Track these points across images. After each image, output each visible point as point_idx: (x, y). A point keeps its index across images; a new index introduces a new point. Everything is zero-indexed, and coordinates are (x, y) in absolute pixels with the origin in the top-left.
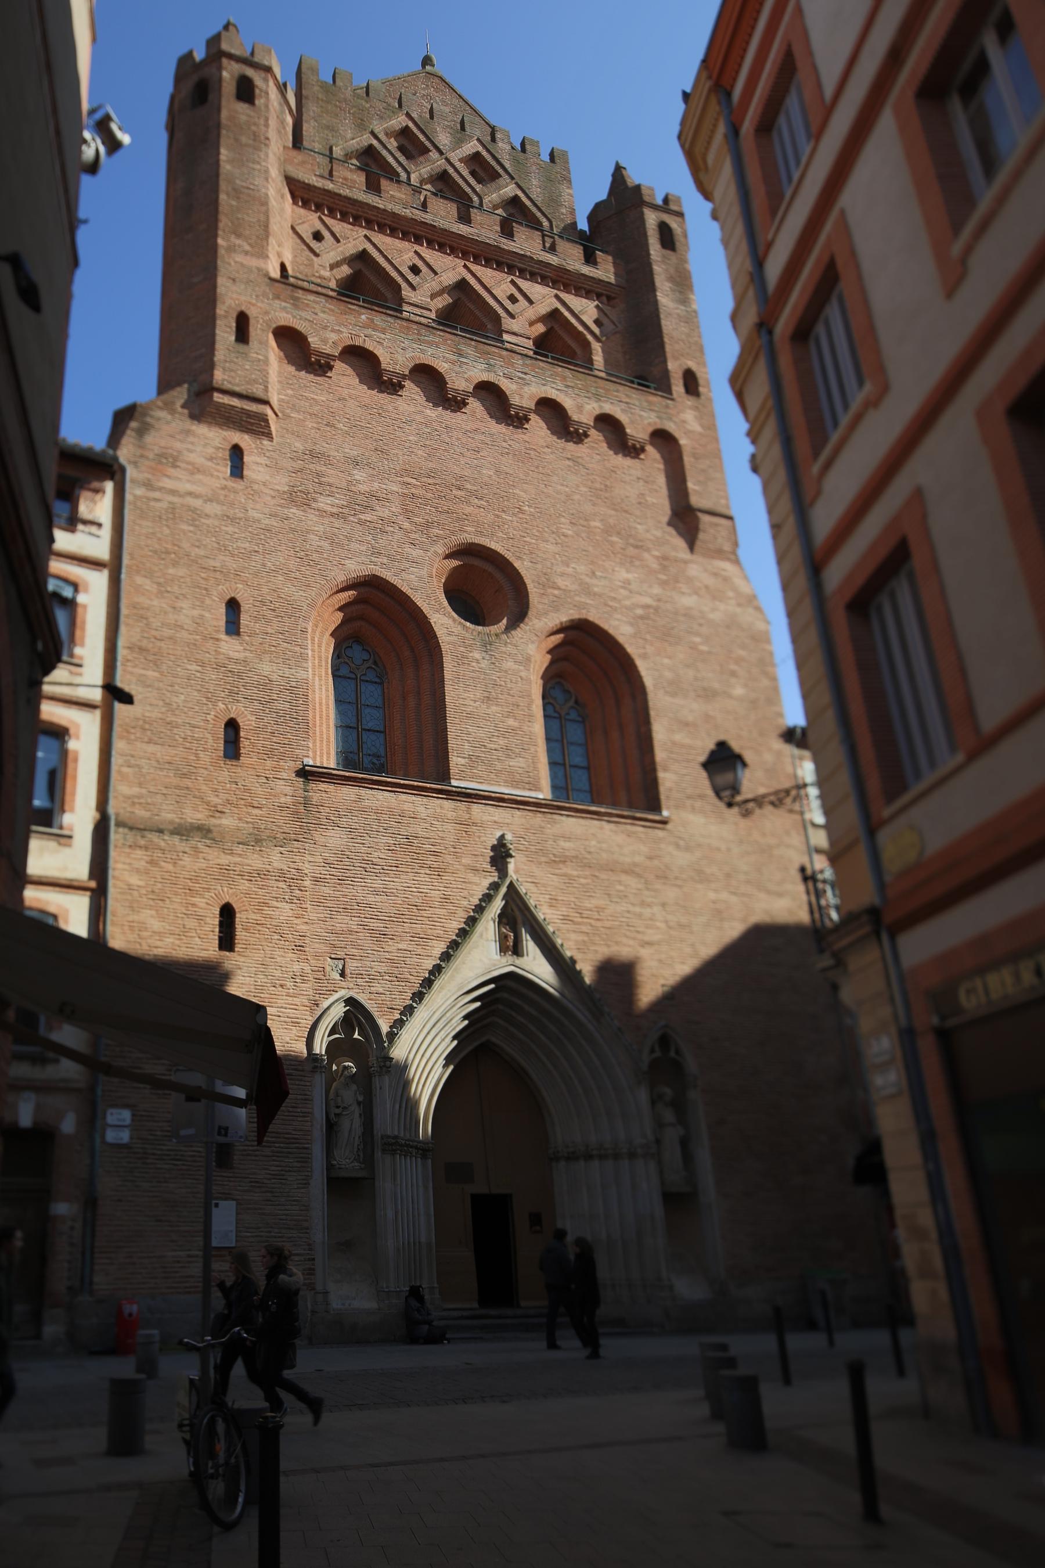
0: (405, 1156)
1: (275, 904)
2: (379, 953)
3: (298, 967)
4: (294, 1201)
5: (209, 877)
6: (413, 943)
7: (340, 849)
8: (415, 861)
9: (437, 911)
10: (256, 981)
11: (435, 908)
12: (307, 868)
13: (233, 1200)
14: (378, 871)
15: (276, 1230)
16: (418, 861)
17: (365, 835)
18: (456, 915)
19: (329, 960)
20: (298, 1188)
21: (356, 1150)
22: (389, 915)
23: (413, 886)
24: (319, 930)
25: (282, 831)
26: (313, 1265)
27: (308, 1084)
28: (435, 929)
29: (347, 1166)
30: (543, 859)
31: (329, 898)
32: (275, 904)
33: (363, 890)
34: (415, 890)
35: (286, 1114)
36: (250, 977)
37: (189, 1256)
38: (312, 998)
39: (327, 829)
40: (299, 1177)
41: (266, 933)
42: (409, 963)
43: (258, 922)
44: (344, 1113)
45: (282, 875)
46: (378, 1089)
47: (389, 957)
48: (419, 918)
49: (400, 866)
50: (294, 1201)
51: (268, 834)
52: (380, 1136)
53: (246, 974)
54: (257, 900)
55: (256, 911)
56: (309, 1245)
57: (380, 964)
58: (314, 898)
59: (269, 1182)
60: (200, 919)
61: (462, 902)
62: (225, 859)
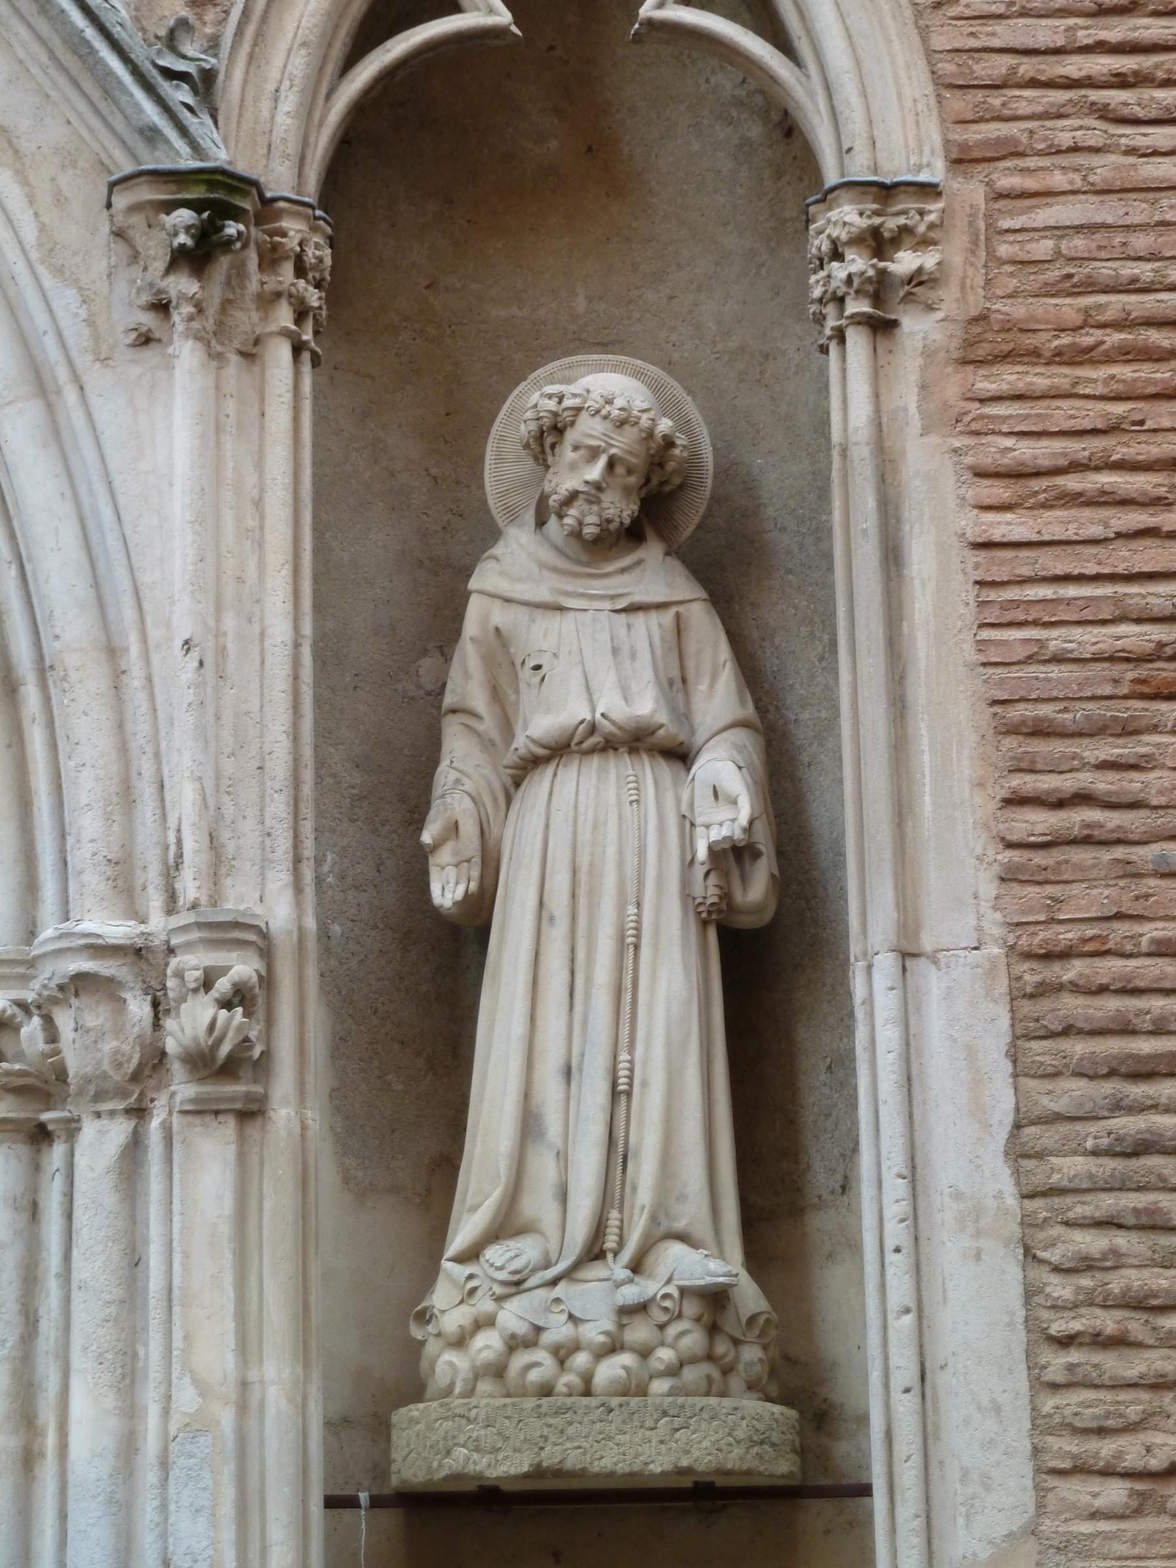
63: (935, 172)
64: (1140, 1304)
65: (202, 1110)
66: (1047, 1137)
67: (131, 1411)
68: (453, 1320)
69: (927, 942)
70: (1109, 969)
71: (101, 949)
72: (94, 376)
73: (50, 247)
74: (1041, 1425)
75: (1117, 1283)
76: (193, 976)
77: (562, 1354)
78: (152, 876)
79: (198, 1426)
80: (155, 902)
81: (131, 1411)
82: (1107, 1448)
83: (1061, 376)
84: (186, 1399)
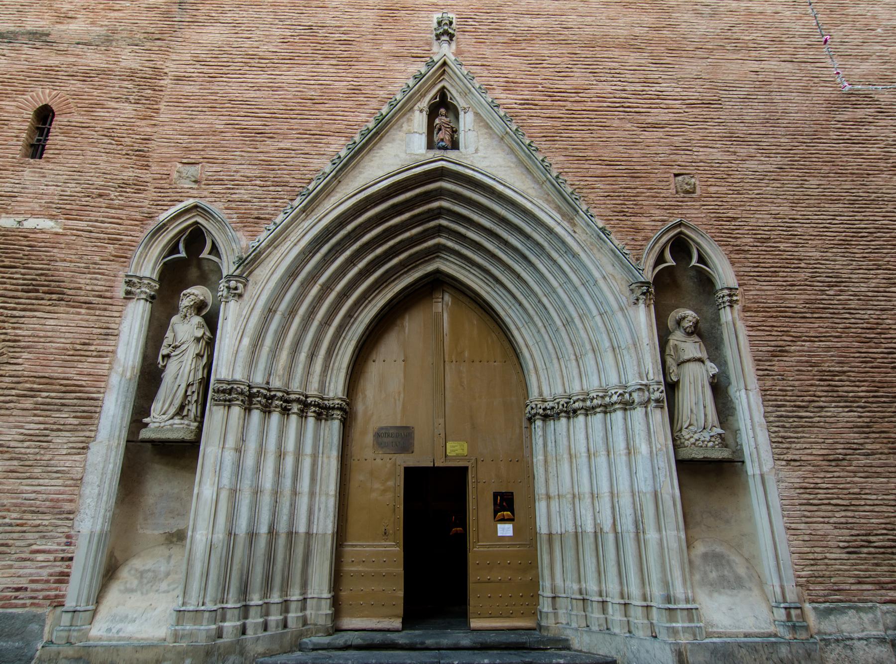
2: (249, 154)
3: (131, 174)
4: (56, 472)
5: (28, 79)
8: (318, 52)
9: (341, 104)
10: (63, 191)
11: (338, 100)
12: (171, 68)
15: (14, 515)
16: (321, 52)
17: (253, 29)
18: (366, 107)
19: (180, 165)
20: (69, 454)
22: (272, 111)
23: (311, 78)
24: (171, 133)
25: (143, 31)
26: (69, 567)
29: (162, 425)
30: (501, 39)
31: (192, 98)
33: (240, 86)
34: (312, 82)
35: (71, 353)
36: (57, 186)
38: (145, 210)
42: (291, 163)
44: (173, 354)
45: (131, 75)
48: (312, 113)
49: (296, 58)
50: (56, 472)
53: (50, 183)
54: (87, 101)
55: (83, 113)
56: (68, 537)
57: (250, 167)
59: (20, 445)
61: (377, 92)
63: (737, 287)
64: (783, 437)
65: (656, 407)
66: (768, 415)
67: (651, 448)
68: (687, 437)
69: (749, 388)
70: (773, 392)
71: (642, 385)
72: (628, 308)
73: (621, 292)
74: (773, 453)
75: (780, 434)
76: (656, 389)
77: (703, 442)
78: (644, 375)
79: (660, 450)
80: (645, 379)
81: (651, 448)
82: (782, 457)
83: (756, 314)
84: (659, 446)
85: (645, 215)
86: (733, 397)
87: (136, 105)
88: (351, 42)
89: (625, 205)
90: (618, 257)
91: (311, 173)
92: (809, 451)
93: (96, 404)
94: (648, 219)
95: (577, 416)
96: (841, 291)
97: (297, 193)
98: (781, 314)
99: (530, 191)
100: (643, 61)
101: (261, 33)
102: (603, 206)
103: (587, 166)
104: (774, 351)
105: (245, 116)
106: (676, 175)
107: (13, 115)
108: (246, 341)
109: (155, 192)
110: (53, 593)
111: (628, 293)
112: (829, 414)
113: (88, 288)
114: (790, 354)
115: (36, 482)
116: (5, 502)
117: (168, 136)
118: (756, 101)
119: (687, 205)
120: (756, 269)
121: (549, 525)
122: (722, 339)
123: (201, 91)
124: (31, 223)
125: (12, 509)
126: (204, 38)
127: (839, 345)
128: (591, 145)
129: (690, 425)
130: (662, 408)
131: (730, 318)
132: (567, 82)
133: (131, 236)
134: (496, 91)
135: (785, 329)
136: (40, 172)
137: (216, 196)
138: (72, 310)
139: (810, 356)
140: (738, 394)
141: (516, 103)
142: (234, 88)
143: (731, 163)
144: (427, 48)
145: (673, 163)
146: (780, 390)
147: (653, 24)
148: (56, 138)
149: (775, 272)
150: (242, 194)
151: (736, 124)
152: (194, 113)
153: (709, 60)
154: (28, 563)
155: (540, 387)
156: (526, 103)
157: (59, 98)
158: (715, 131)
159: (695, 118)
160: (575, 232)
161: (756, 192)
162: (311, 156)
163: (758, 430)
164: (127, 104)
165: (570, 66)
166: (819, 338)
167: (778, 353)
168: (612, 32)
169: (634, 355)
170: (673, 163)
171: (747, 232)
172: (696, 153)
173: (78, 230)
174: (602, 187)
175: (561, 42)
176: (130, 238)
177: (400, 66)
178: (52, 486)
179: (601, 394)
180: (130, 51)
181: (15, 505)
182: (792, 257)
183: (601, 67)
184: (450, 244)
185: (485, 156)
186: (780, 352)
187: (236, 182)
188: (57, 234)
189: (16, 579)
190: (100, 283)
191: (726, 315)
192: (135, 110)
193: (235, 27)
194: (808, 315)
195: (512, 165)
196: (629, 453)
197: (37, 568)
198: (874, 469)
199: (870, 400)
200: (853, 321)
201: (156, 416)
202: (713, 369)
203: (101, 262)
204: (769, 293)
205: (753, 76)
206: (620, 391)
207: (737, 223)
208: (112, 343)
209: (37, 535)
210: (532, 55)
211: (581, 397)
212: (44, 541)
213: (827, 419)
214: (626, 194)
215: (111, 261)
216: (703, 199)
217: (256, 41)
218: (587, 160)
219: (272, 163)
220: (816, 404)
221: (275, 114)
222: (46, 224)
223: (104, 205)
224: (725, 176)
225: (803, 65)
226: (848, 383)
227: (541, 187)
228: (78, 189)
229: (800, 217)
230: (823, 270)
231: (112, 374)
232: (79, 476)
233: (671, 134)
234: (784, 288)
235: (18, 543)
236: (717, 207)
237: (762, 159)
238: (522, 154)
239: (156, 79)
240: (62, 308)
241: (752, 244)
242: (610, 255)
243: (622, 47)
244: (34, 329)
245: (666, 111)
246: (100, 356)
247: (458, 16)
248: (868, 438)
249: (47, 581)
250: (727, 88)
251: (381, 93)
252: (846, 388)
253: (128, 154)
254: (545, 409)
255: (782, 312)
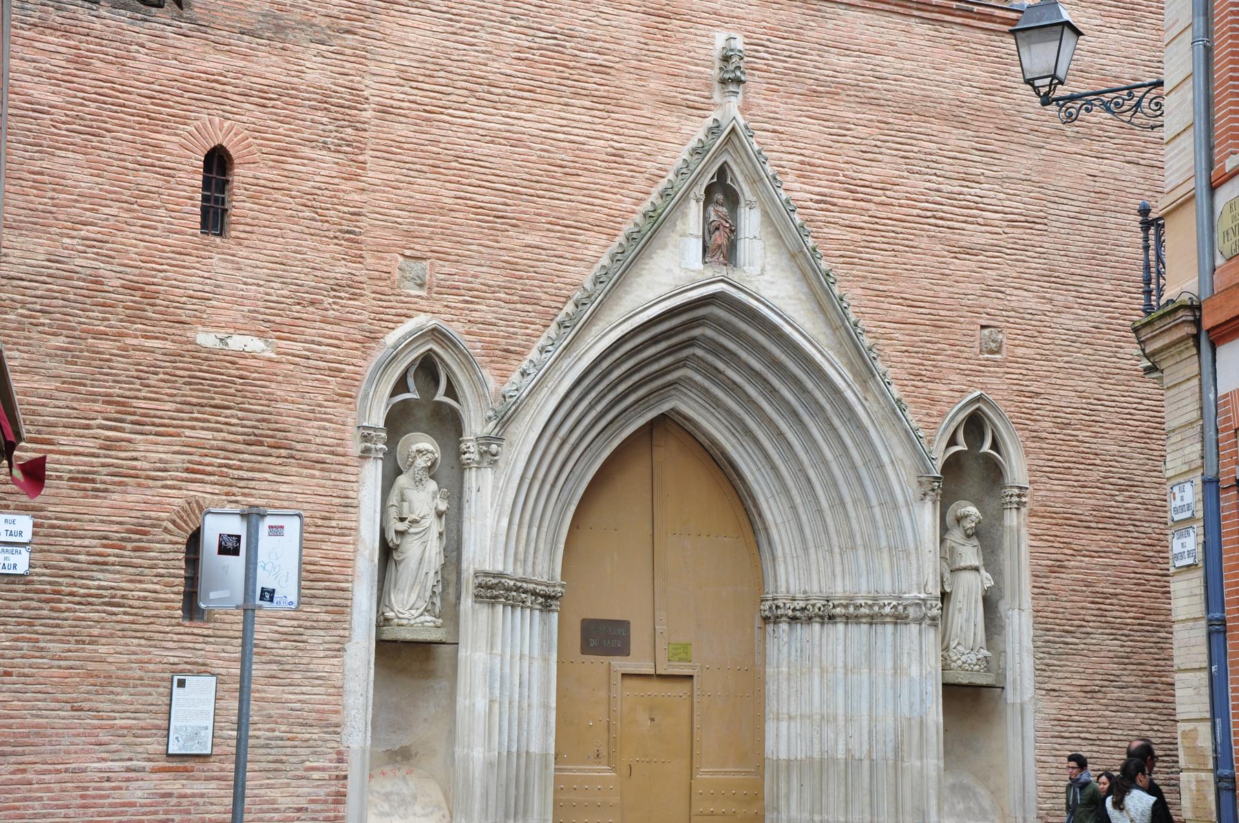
0: (512, 606)
1: (307, 152)
2: (490, 251)
3: (343, 270)
4: (317, 678)
6: (552, 234)
7: (428, 53)
11: (596, 171)
12: (369, 87)
13: (213, 675)
14: (496, 98)
15: (283, 728)
16: (570, 82)
17: (477, 28)
19: (401, 259)
20: (326, 657)
21: (429, 593)
22: (513, 181)
23: (559, 129)
25: (323, 11)
26: (344, 786)
27: (352, 478)
28: (593, 211)
29: (412, 622)
31: (406, 146)
32: (307, 152)
33: (469, 133)
34: (561, 136)
36: (259, 285)
37: (128, 770)
38: (366, 326)
39: (407, 12)
40: (327, 639)
41: (289, 206)
43: (276, 185)
44: (412, 530)
45: (324, 101)
46: (474, 490)
47: (507, 258)
48: (564, 190)
49: (538, 90)
50: (317, 678)
51: (299, 18)
52: (472, 572)
53: (249, 280)
55: (271, 163)
56: (339, 753)
57: (492, 270)
58: (378, 144)
59: (275, 645)
60: (168, 173)
62: (215, 62)
64: (1047, 665)
65: (930, 625)
66: (1036, 639)
67: (921, 670)
71: (920, 599)
72: (914, 504)
74: (1036, 682)
75: (1045, 661)
79: (930, 673)
83: (1041, 520)
84: (929, 669)
85: (944, 381)
86: (1003, 615)
87: (336, 155)
88: (608, 70)
89: (923, 365)
90: (912, 440)
91: (568, 287)
92: (1068, 681)
93: (345, 596)
94: (945, 387)
95: (836, 623)
96: (1131, 497)
97: (552, 317)
98: (1067, 522)
99: (821, 338)
100: (966, 144)
101: (488, 36)
102: (899, 365)
103: (886, 306)
104: (1053, 566)
105: (479, 186)
106: (983, 327)
107: (179, 159)
108: (505, 522)
109: (374, 299)
110: (332, 814)
111: (915, 485)
112: (1094, 641)
113: (318, 440)
114: (1068, 571)
115: (298, 689)
116: (272, 712)
117: (382, 210)
118: (1086, 223)
119: (989, 372)
120: (1050, 464)
121: (789, 750)
122: (1001, 543)
123: (418, 135)
124: (237, 342)
125: (279, 720)
126: (412, 37)
127: (1116, 563)
128: (895, 274)
129: (959, 644)
130: (936, 626)
131: (1015, 523)
132: (874, 170)
133: (353, 365)
134: (790, 177)
135: (1067, 540)
136: (232, 262)
137: (453, 312)
138: (306, 471)
139: (1086, 574)
140: (1010, 612)
141: (811, 200)
142: (459, 134)
143: (1045, 315)
144: (706, 94)
145: (981, 310)
146: (1052, 612)
147: (986, 83)
148: (240, 204)
149: (1069, 468)
150: (484, 311)
151: (1059, 258)
152: (411, 173)
153: (1044, 151)
154: (304, 782)
155: (787, 581)
156: (824, 201)
157: (236, 135)
158: (1034, 265)
159: (1015, 243)
160: (866, 399)
161: (1066, 359)
162: (566, 261)
163: (1025, 655)
164: (324, 152)
165: (878, 143)
166: (1099, 553)
167: (1056, 569)
168: (934, 91)
169: (914, 562)
170: (981, 310)
171: (1048, 413)
172: (1009, 298)
173: (294, 355)
174: (901, 338)
175: (874, 102)
176: (352, 367)
177: (671, 120)
178: (316, 694)
179: (870, 602)
180: (315, 53)
181: (282, 716)
182: (1089, 450)
183: (916, 149)
184: (698, 378)
185: (773, 280)
186: (1058, 567)
187: (475, 293)
188: (270, 360)
189: (295, 799)
190: (330, 433)
191: (1012, 519)
192: (337, 163)
193: (451, 20)
194: (1093, 525)
195: (803, 297)
196: (895, 673)
197: (313, 787)
198: (1125, 703)
199: (1135, 627)
200: (1136, 534)
201: (401, 610)
202: (989, 583)
203: (326, 403)
204: (1058, 494)
205: (1089, 181)
206: (894, 603)
207: (1039, 401)
208: (353, 517)
209: (308, 751)
210: (835, 118)
211: (844, 602)
212: (315, 758)
213: (1092, 647)
214: (926, 350)
215: (335, 401)
216: (1008, 364)
217: (483, 52)
218: (887, 297)
219: (519, 267)
220: (1084, 630)
221: (516, 186)
222: (255, 344)
223: (318, 318)
224: (1036, 334)
225: (1150, 170)
226: (1117, 608)
227: (834, 332)
228: (284, 292)
229: (1106, 397)
230: (1117, 470)
231: (358, 557)
232: (340, 684)
233: (985, 265)
234: (1074, 489)
235: (292, 759)
236: (1021, 377)
237: (1080, 311)
238: (816, 284)
239: (355, 108)
240: (294, 469)
241: (1050, 430)
242: (902, 434)
243: (943, 118)
244: (268, 497)
245: (984, 228)
246: (343, 535)
247: (747, 40)
248: (1125, 669)
249: (325, 802)
250: (1057, 199)
251: (649, 164)
252: (1114, 614)
253: (336, 237)
254: (794, 610)
255: (1069, 520)
